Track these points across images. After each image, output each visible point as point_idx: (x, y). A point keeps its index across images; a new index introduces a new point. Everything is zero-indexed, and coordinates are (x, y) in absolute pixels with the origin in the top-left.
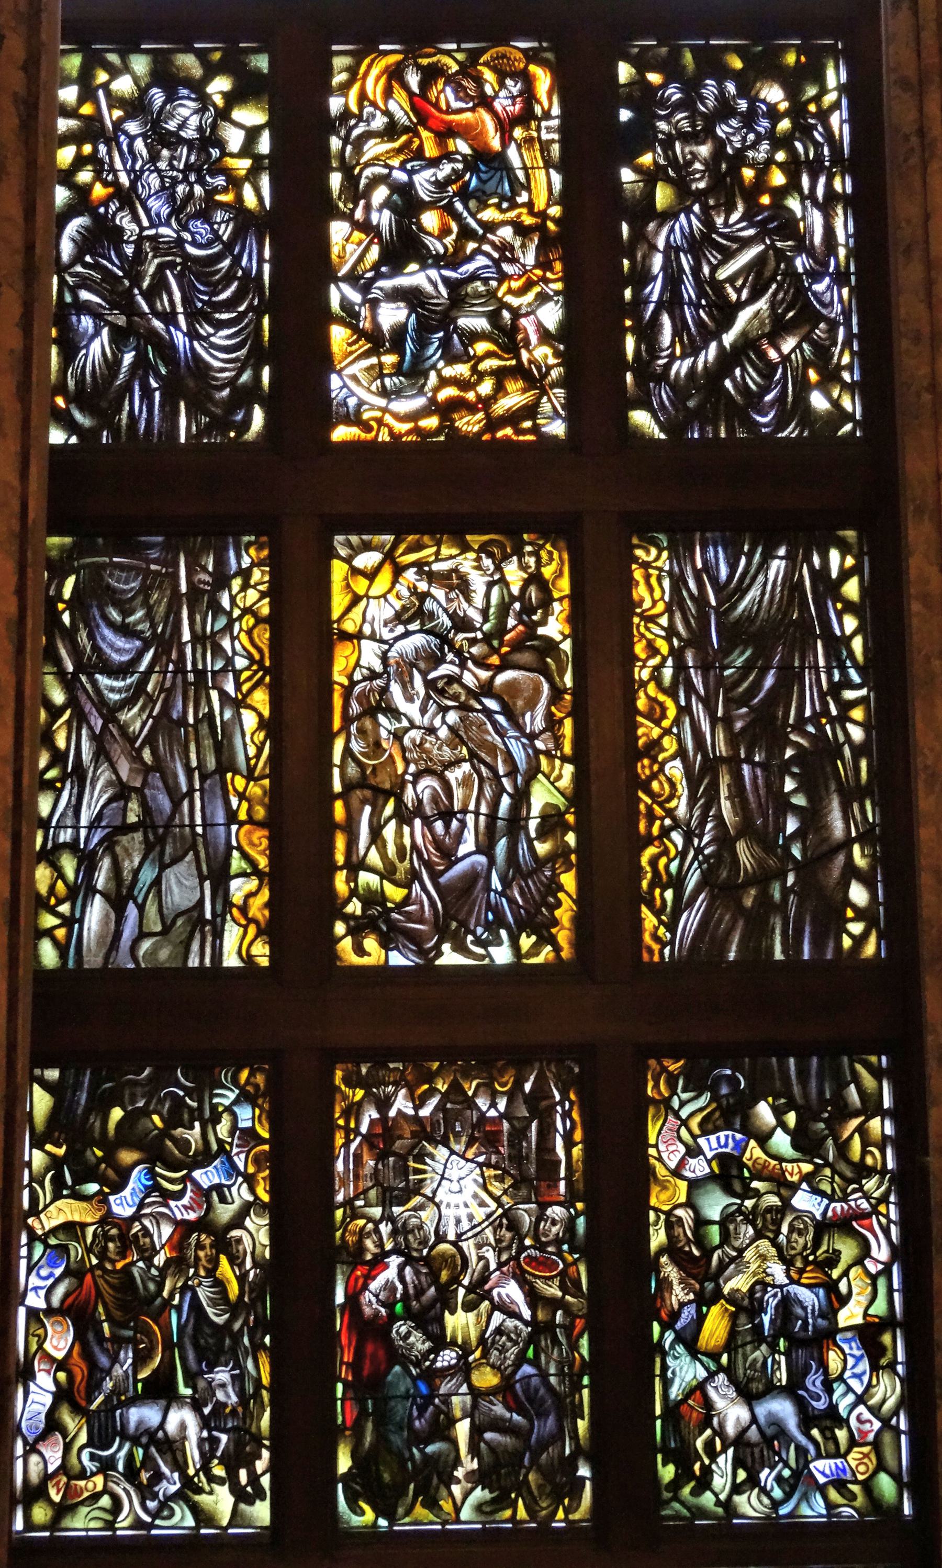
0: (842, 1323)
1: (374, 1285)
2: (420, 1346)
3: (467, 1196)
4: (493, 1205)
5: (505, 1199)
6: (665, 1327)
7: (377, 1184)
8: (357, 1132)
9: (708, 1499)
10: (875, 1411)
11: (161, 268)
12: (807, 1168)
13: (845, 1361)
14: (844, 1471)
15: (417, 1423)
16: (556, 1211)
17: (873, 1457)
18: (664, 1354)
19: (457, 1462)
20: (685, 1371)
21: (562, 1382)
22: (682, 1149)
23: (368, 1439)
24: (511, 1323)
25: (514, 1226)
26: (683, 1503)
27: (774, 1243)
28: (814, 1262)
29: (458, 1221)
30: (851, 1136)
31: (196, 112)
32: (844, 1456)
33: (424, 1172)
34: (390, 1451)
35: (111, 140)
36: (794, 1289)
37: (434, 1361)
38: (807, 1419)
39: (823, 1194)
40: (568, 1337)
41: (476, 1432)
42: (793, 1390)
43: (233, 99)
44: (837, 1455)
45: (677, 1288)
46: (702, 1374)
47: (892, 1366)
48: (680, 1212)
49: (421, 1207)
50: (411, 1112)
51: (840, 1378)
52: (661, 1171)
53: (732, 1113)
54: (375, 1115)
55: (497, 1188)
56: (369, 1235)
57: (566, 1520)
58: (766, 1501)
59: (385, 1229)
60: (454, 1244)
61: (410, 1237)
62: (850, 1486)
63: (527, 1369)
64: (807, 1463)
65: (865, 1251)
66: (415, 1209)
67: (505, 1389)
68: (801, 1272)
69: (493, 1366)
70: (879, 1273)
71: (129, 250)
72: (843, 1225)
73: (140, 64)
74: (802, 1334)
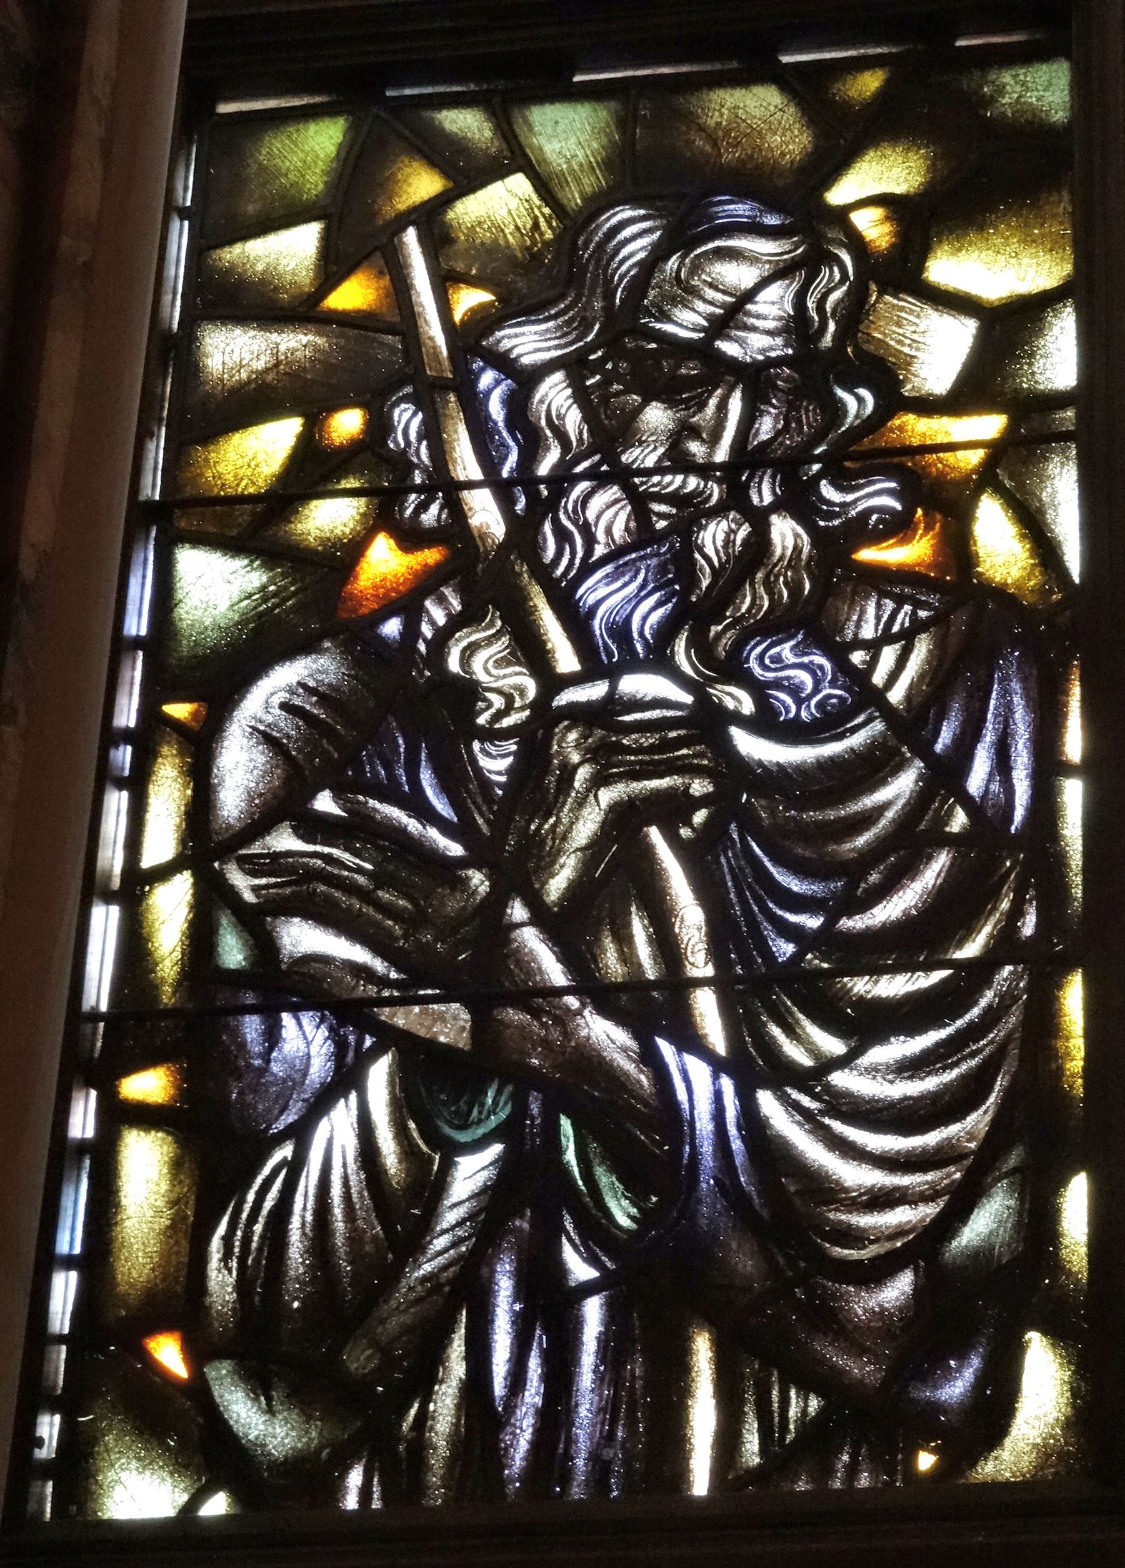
11: (624, 822)
31: (781, 272)
35: (445, 389)
43: (922, 221)
71: (495, 763)
73: (568, 134)
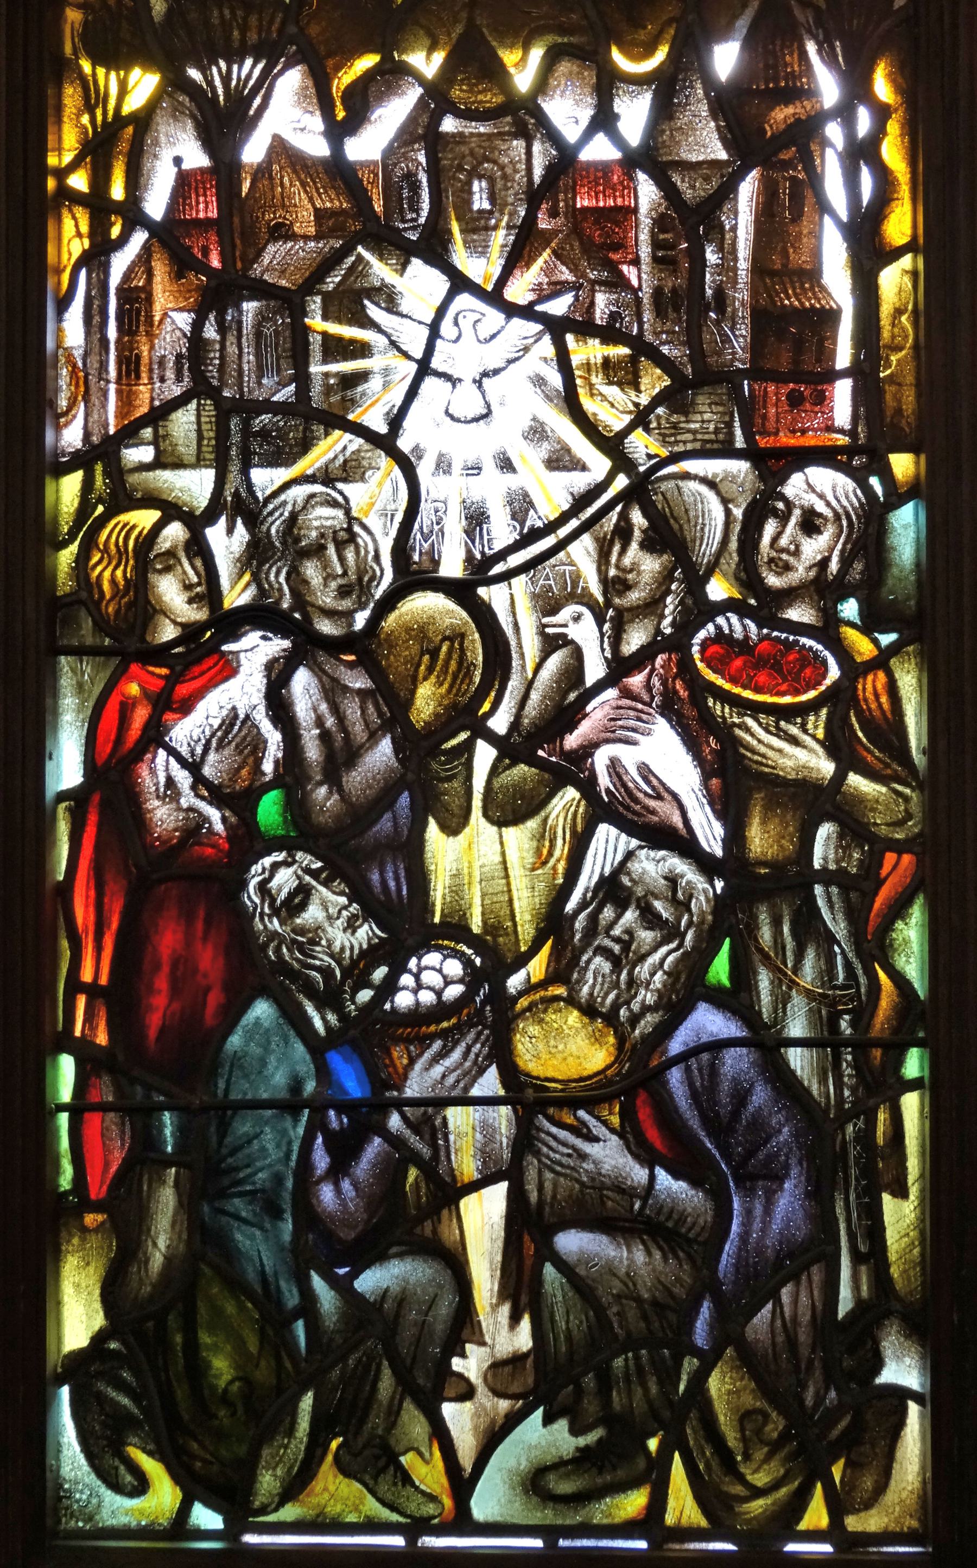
1: (186, 731)
2: (338, 936)
3: (506, 431)
4: (599, 465)
5: (641, 445)
7: (201, 389)
8: (133, 215)
15: (327, 1194)
16: (820, 487)
19: (464, 1328)
21: (829, 1068)
23: (162, 1241)
24: (653, 866)
25: (667, 536)
29: (476, 519)
33: (364, 350)
34: (235, 1285)
37: (390, 987)
40: (856, 917)
41: (528, 1228)
49: (351, 470)
50: (318, 147)
54: (196, 157)
55: (610, 407)
56: (169, 560)
57: (835, 1532)
59: (226, 542)
60: (461, 591)
61: (311, 570)
63: (709, 1022)
66: (326, 477)
67: (632, 1087)
69: (590, 1011)
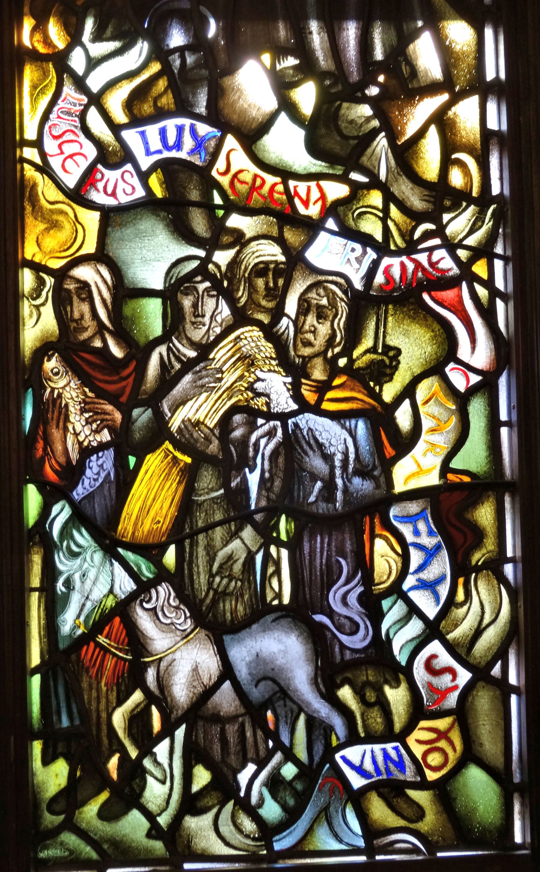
0: (399, 487)
6: (51, 495)
9: (133, 825)
10: (460, 651)
12: (337, 191)
13: (405, 558)
14: (400, 765)
17: (456, 736)
18: (49, 549)
20: (93, 579)
22: (91, 152)
26: (83, 834)
27: (270, 333)
28: (349, 370)
30: (421, 134)
32: (402, 737)
36: (307, 420)
38: (329, 673)
39: (366, 240)
42: (301, 613)
44: (388, 735)
45: (77, 421)
46: (125, 585)
47: (494, 566)
48: (84, 272)
51: (396, 590)
52: (47, 191)
53: (192, 84)
58: (249, 825)
62: (412, 793)
64: (330, 752)
65: (448, 350)
68: (322, 388)
70: (472, 391)
72: (408, 298)
74: (323, 507)
